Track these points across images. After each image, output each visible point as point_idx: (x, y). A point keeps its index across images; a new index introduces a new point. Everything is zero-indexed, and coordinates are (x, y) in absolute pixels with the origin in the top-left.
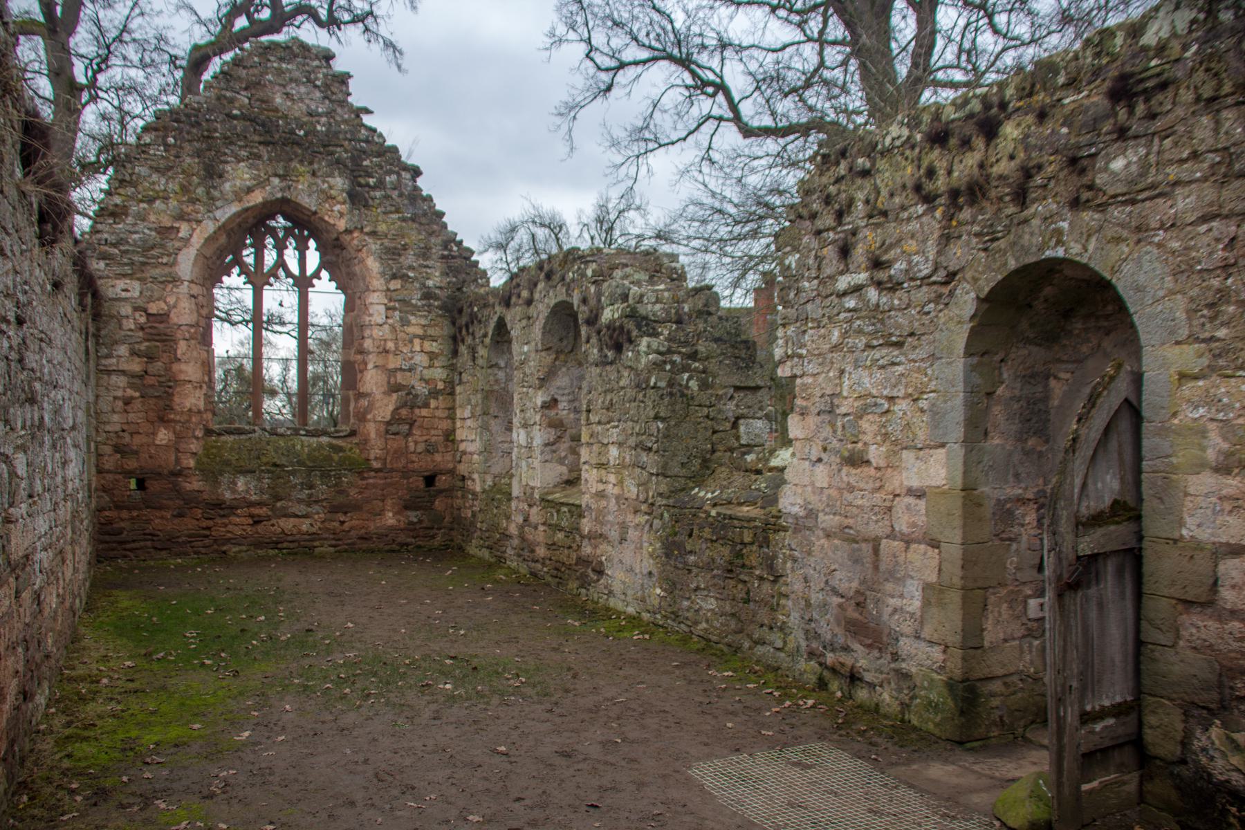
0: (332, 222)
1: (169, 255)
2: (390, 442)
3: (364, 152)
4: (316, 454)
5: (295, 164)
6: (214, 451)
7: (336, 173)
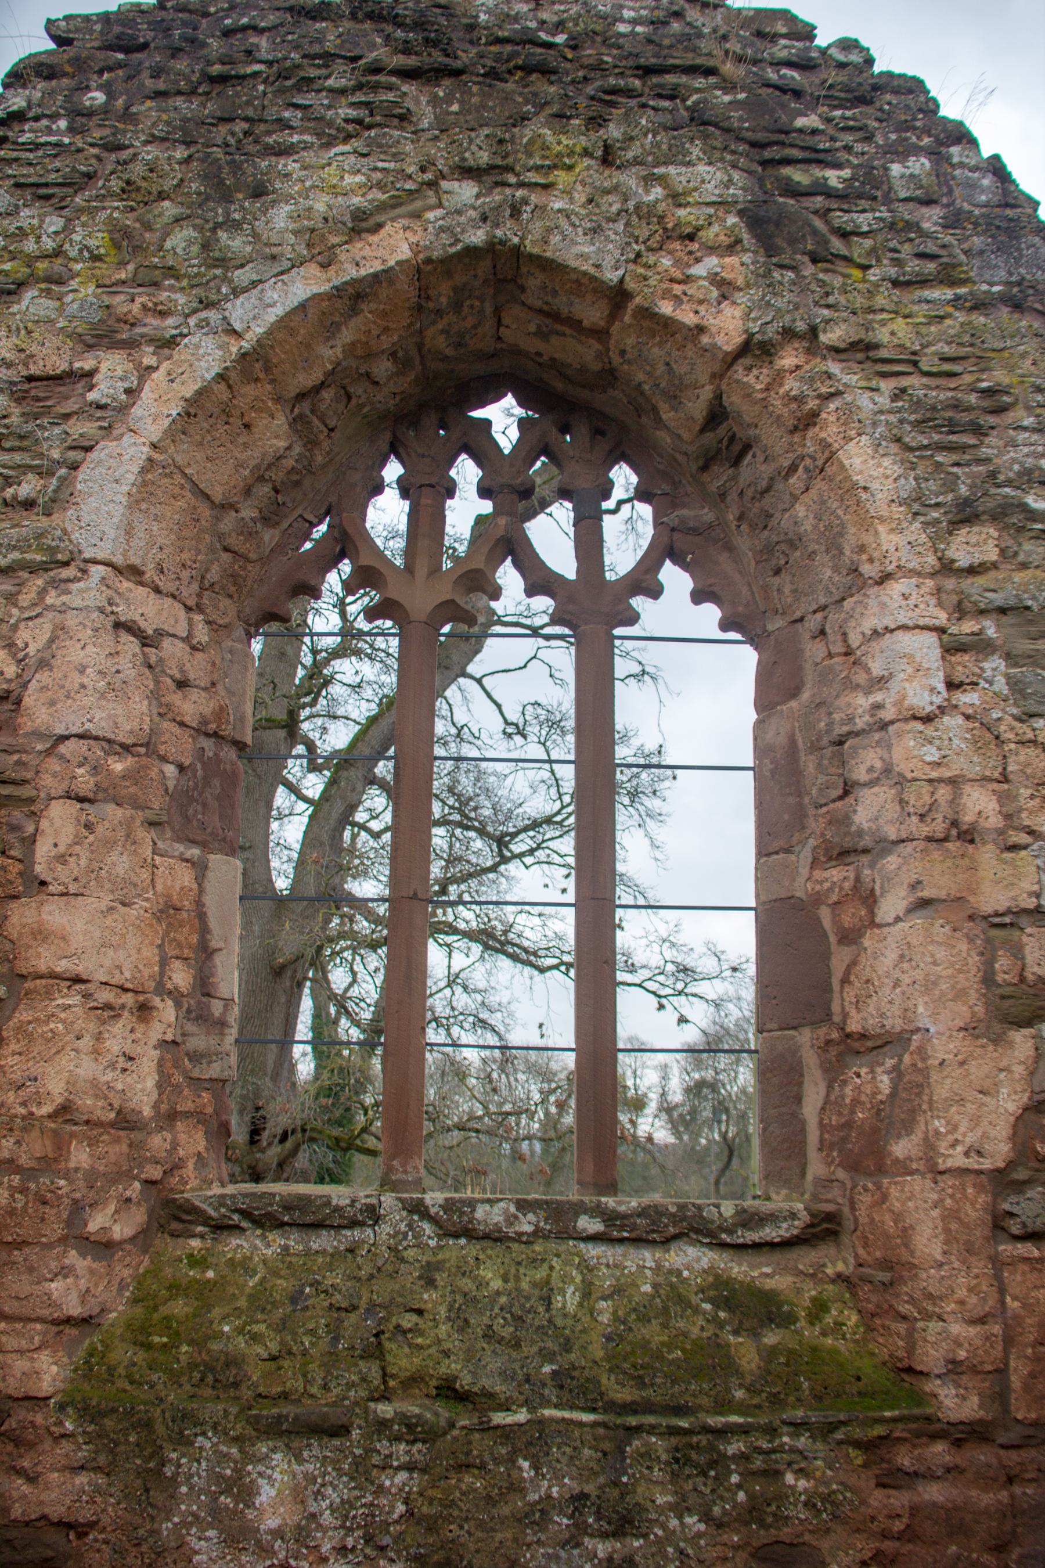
0: (688, 318)
1: (44, 473)
2: (1016, 1279)
3: (797, 94)
4: (653, 1333)
5: (540, 129)
6: (179, 1308)
7: (696, 152)
